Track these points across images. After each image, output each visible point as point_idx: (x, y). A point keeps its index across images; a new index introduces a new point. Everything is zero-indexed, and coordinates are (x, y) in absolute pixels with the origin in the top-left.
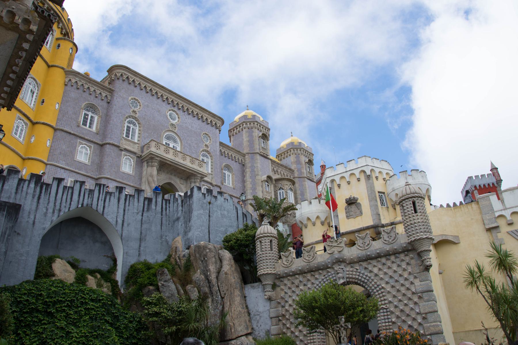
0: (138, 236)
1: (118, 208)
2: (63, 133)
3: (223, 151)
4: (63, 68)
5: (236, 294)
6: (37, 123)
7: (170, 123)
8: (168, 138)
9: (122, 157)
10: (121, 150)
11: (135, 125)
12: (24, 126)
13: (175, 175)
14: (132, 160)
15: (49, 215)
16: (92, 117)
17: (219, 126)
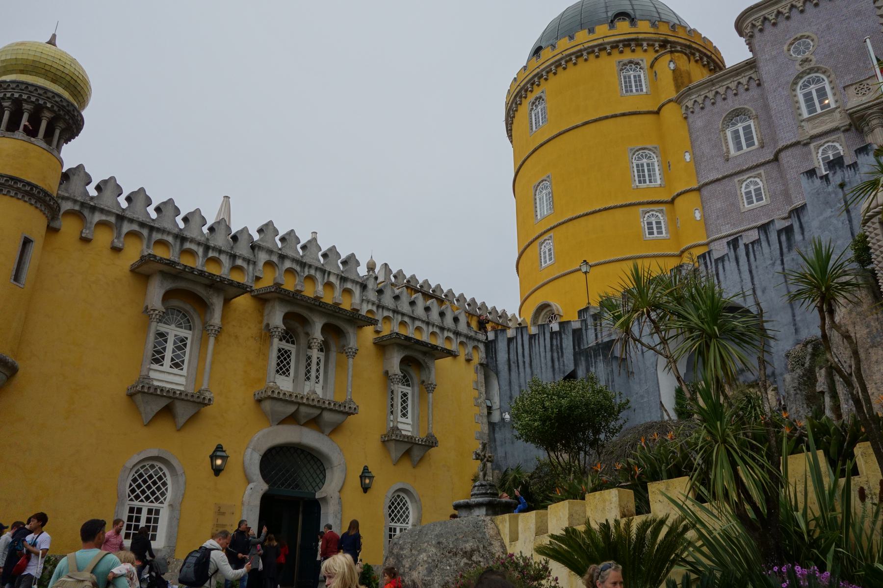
1: (740, 273)
2: (709, 187)
4: (670, 101)
9: (814, 154)
10: (807, 144)
11: (819, 80)
12: (660, 215)
14: (837, 145)
16: (744, 129)
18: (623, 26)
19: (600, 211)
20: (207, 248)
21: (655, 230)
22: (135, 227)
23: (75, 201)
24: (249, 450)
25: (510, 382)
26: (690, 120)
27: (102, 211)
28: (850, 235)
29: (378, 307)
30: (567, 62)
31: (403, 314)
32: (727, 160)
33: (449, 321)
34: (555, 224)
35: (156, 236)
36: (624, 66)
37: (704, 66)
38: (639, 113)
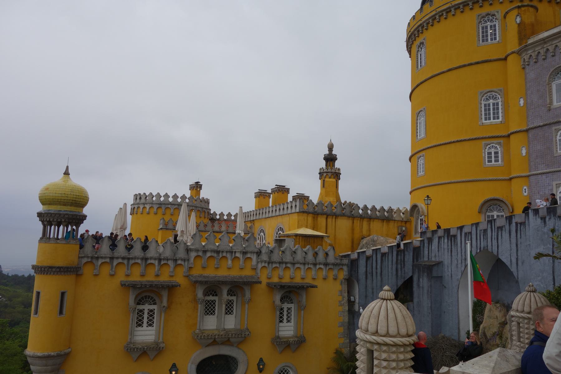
4: (513, 53)
6: (509, 136)
15: (459, 266)
19: (454, 142)
20: (160, 260)
21: (493, 159)
22: (120, 260)
23: (88, 257)
24: (189, 365)
25: (366, 286)
26: (527, 71)
27: (102, 258)
28: (552, 272)
29: (269, 263)
31: (286, 263)
33: (321, 257)
35: (132, 262)
36: (482, 18)
38: (490, 61)
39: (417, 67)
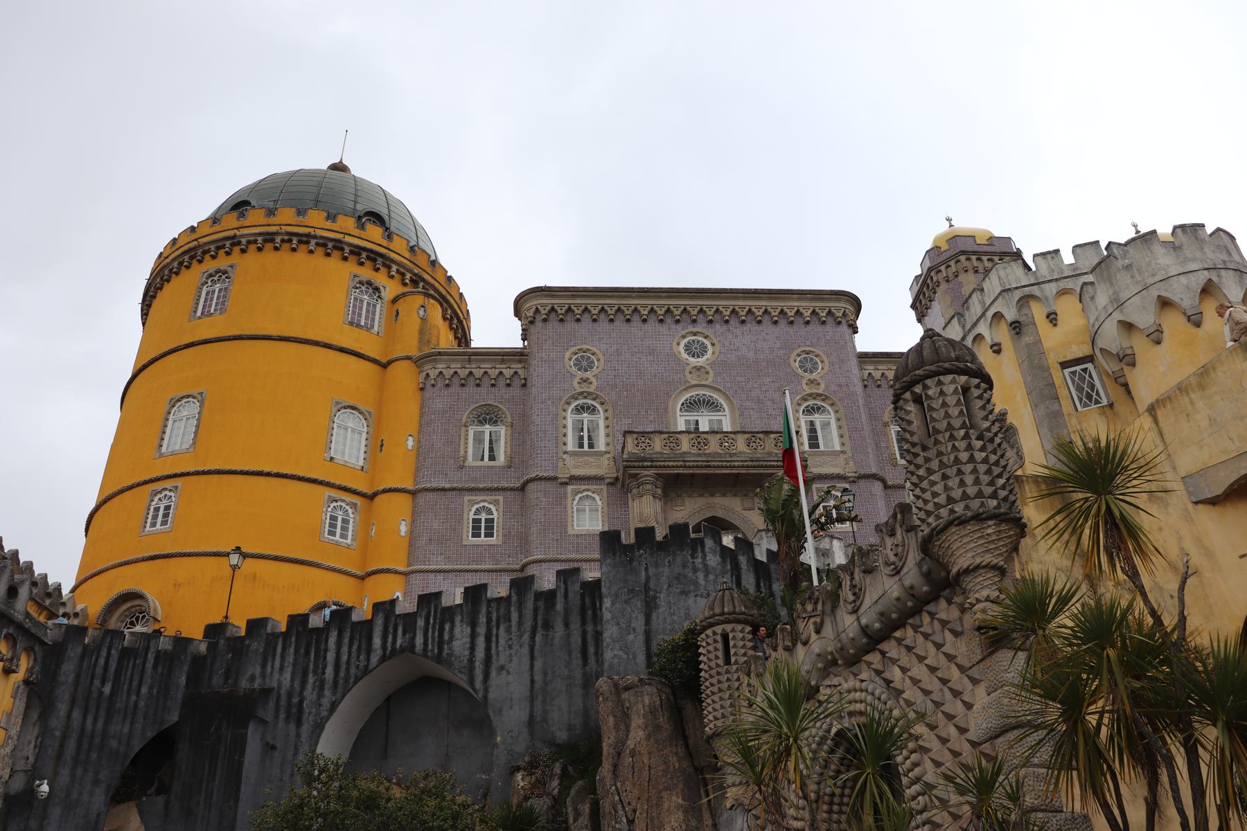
0: (525, 691)
1: (473, 636)
2: (430, 495)
3: (877, 374)
4: (408, 358)
5: (666, 806)
7: (688, 369)
8: (691, 405)
9: (570, 499)
10: (566, 484)
11: (593, 410)
12: (350, 511)
13: (724, 495)
14: (597, 498)
15: (327, 693)
17: (844, 315)
18: (374, 233)
19: (268, 474)
21: (338, 531)
26: (429, 392)
30: (283, 241)
32: (462, 467)
34: (192, 469)
37: (451, 329)
39: (195, 312)
